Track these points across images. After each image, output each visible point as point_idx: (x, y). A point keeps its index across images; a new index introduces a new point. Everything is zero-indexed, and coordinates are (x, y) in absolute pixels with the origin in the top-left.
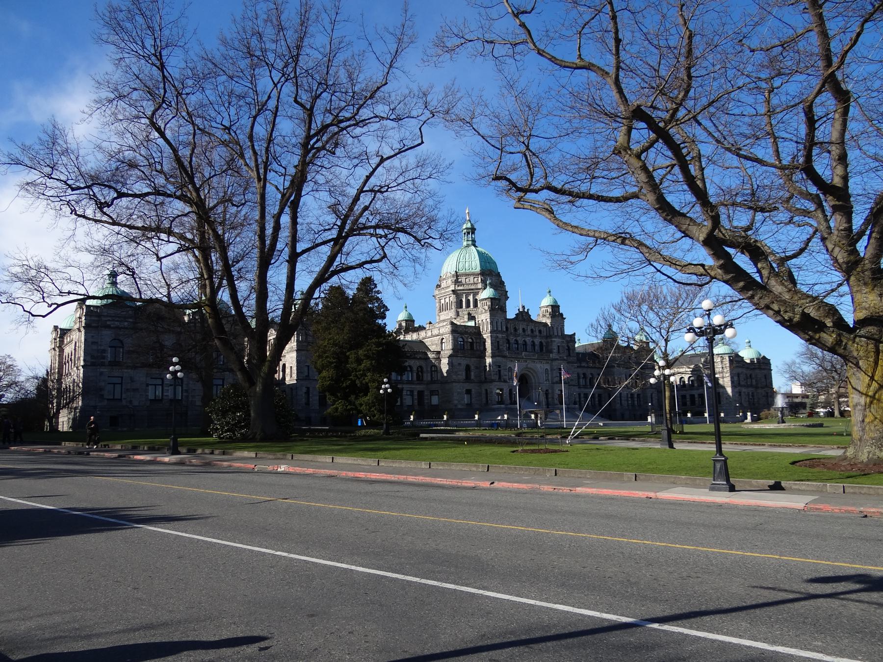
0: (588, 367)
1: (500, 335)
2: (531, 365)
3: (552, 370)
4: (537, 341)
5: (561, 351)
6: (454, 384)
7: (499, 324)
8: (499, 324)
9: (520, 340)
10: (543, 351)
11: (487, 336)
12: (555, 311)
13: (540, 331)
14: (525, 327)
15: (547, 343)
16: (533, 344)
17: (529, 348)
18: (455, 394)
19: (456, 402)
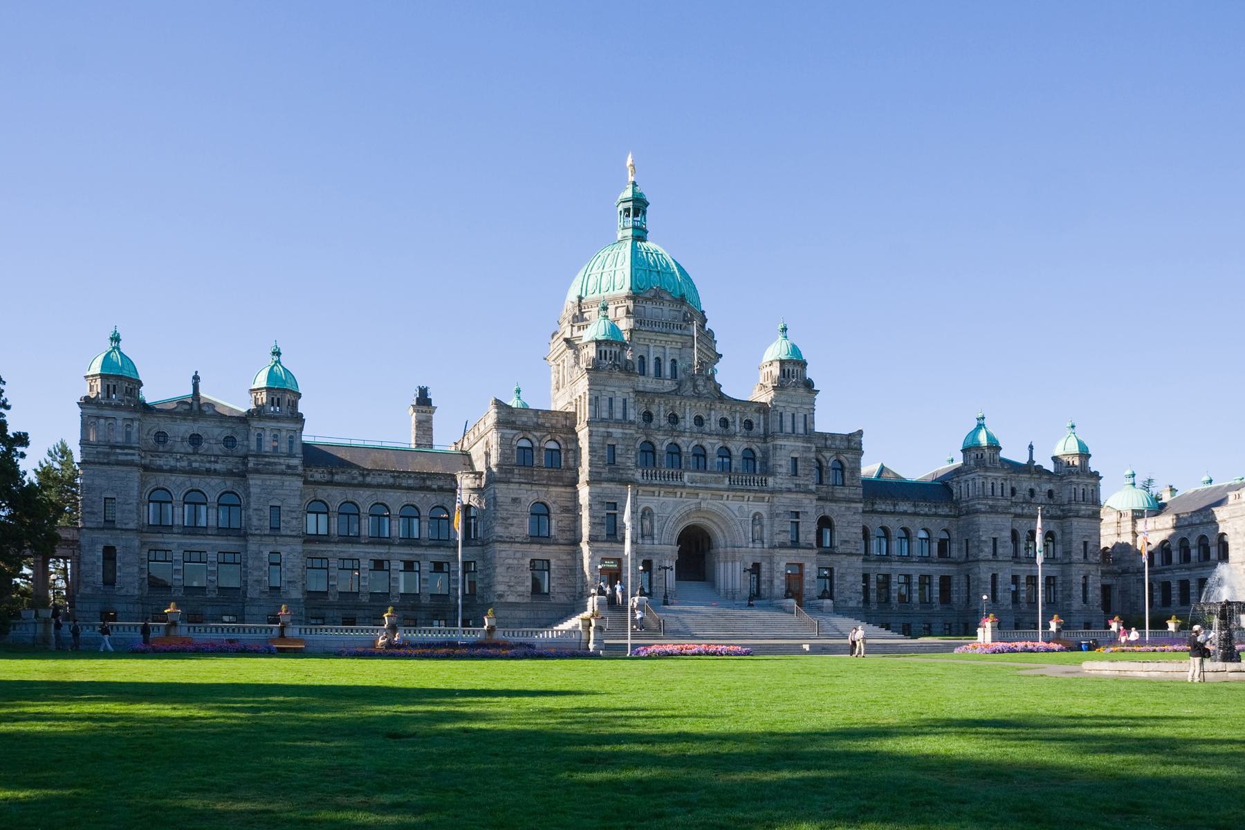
0: (916, 514)
1: (617, 431)
2: (709, 502)
3: (773, 515)
4: (737, 447)
5: (799, 472)
6: (498, 547)
7: (618, 405)
8: (618, 405)
9: (687, 444)
10: (753, 468)
11: (583, 434)
12: (793, 374)
13: (749, 425)
15: (765, 453)
16: (725, 452)
18: (498, 570)
19: (500, 588)
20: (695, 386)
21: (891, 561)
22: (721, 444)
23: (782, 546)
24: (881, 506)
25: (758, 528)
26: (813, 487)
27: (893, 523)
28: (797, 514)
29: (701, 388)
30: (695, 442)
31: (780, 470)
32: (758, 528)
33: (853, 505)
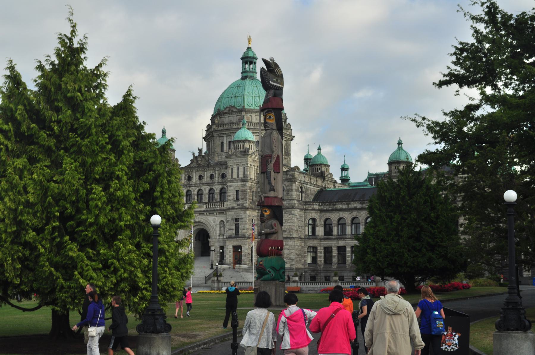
4: (217, 188)
5: (240, 197)
13: (223, 176)
14: (201, 173)
17: (206, 198)
20: (197, 161)
21: (344, 239)
22: (209, 188)
23: (230, 237)
24: (339, 206)
25: (222, 228)
26: (246, 205)
27: (348, 216)
28: (237, 220)
29: (199, 162)
30: (198, 189)
31: (229, 198)
32: (222, 228)
33: (287, 210)
